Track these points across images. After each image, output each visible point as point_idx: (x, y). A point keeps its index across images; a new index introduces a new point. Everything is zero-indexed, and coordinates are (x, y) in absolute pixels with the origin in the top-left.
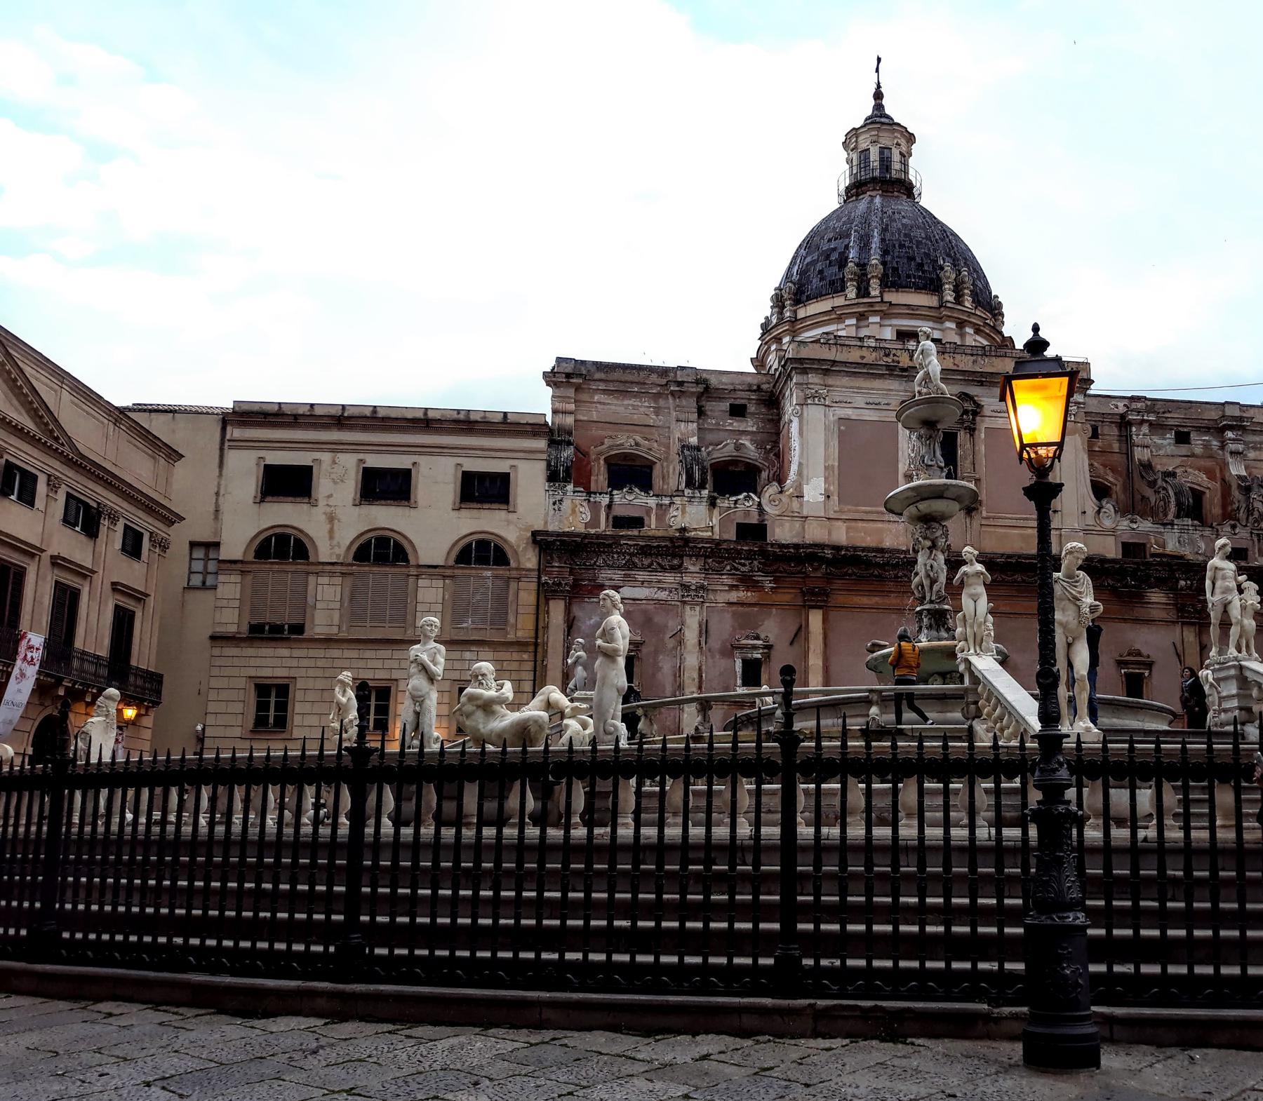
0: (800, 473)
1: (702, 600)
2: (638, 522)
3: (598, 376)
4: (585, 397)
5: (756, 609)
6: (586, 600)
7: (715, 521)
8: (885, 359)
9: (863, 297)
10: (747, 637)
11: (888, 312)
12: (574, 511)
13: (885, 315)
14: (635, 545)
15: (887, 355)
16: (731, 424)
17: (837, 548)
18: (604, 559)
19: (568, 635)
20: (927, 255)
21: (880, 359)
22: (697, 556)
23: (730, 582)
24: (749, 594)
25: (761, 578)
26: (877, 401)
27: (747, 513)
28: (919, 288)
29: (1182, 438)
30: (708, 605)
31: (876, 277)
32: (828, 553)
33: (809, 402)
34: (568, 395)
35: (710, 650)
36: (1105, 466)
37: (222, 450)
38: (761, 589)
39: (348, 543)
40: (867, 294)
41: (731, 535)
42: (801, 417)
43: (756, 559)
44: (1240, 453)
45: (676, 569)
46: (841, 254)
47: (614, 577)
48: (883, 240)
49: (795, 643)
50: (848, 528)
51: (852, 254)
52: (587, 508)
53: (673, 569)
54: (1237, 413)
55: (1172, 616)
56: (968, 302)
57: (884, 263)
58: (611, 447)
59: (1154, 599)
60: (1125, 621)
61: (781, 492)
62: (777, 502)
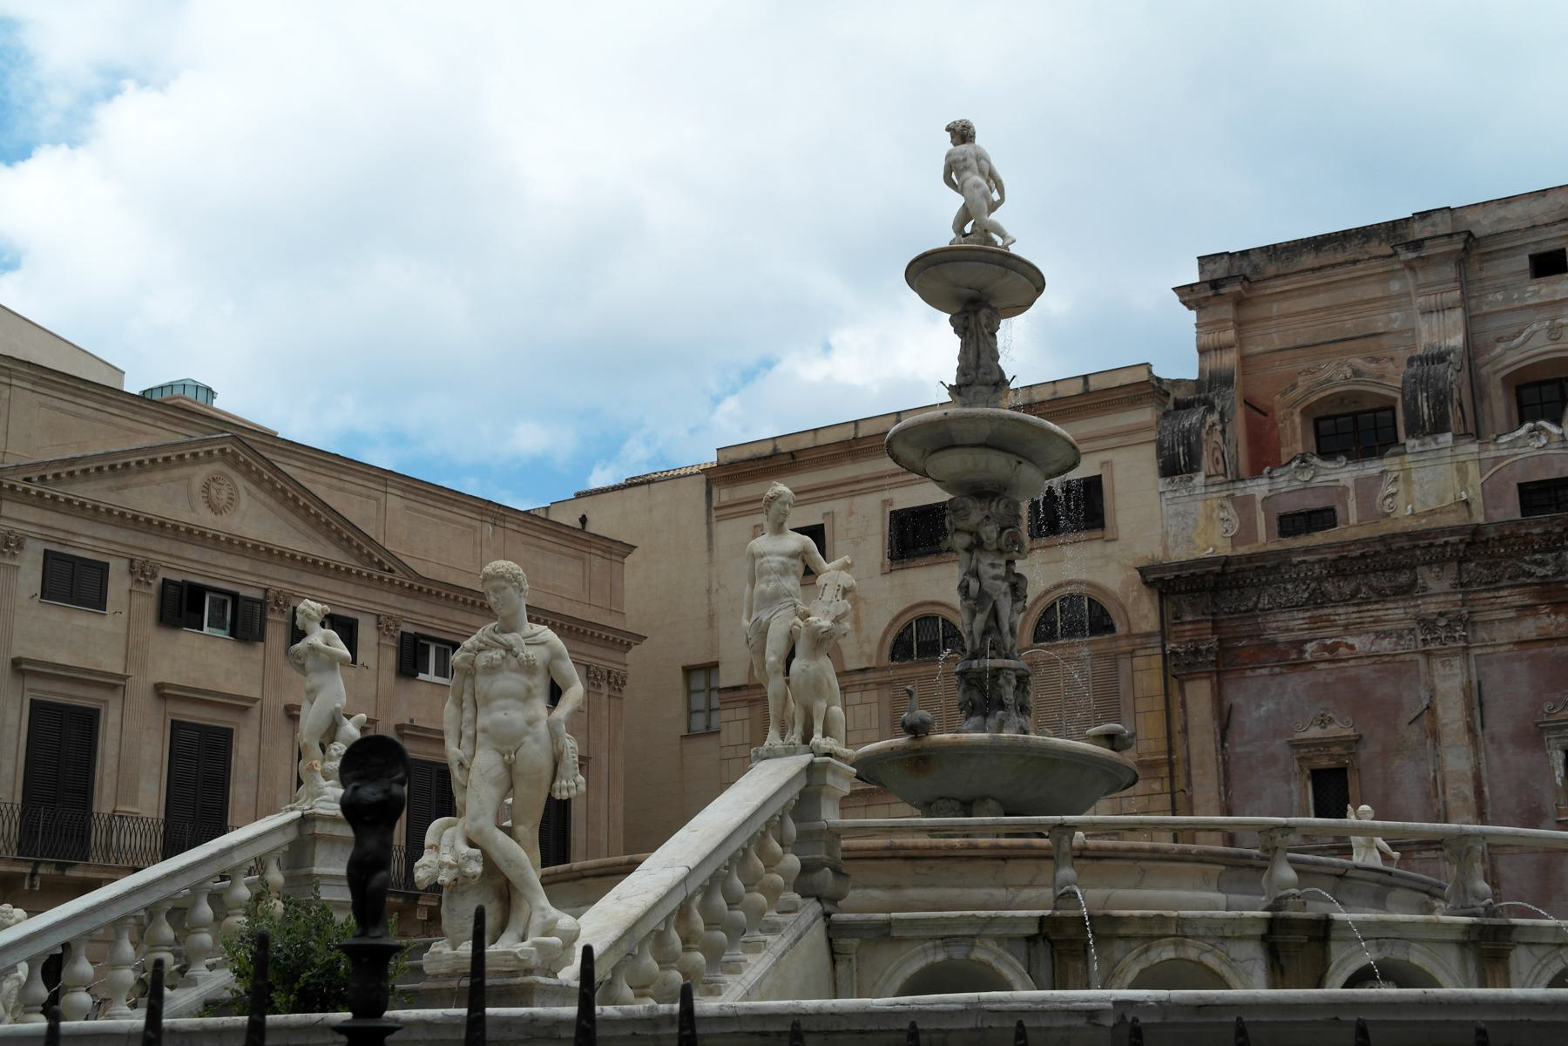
1: (1462, 644)
2: (1323, 518)
3: (1271, 270)
4: (1249, 313)
6: (1249, 673)
7: (1474, 493)
12: (1209, 518)
14: (1320, 561)
16: (1536, 293)
18: (1270, 596)
19: (1224, 738)
22: (1441, 561)
23: (1517, 600)
30: (1478, 651)
34: (1224, 317)
35: (1492, 740)
37: (709, 523)
39: (880, 634)
41: (1510, 509)
45: (1404, 593)
52: (1232, 510)
53: (1406, 591)
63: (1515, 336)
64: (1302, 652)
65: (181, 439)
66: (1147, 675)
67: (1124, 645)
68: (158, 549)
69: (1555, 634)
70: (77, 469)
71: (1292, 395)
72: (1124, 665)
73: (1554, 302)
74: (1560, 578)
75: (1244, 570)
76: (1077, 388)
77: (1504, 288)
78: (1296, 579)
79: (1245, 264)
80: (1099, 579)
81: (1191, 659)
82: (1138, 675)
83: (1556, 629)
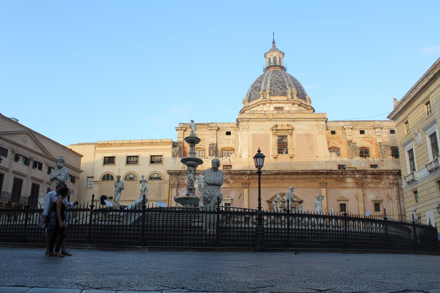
0: (241, 150)
5: (228, 189)
8: (265, 117)
10: (226, 197)
11: (271, 102)
12: (179, 164)
13: (270, 103)
15: (266, 116)
16: (226, 137)
17: (252, 171)
20: (283, 86)
21: (264, 117)
24: (227, 185)
25: (230, 180)
28: (281, 95)
29: (362, 132)
31: (268, 93)
32: (249, 172)
33: (243, 130)
36: (338, 142)
38: (229, 183)
40: (266, 98)
42: (241, 134)
44: (380, 136)
46: (259, 88)
48: (271, 83)
49: (240, 198)
51: (262, 87)
54: (379, 124)
55: (355, 185)
56: (295, 98)
59: (348, 181)
60: (339, 188)
61: (236, 156)
62: (234, 159)
63: (223, 143)
65: (21, 130)
66: (166, 187)
67: (163, 182)
68: (16, 148)
69: (225, 187)
70: (6, 133)
72: (163, 185)
73: (228, 139)
76: (160, 141)
77: (222, 136)
80: (160, 171)
81: (173, 185)
82: (165, 187)
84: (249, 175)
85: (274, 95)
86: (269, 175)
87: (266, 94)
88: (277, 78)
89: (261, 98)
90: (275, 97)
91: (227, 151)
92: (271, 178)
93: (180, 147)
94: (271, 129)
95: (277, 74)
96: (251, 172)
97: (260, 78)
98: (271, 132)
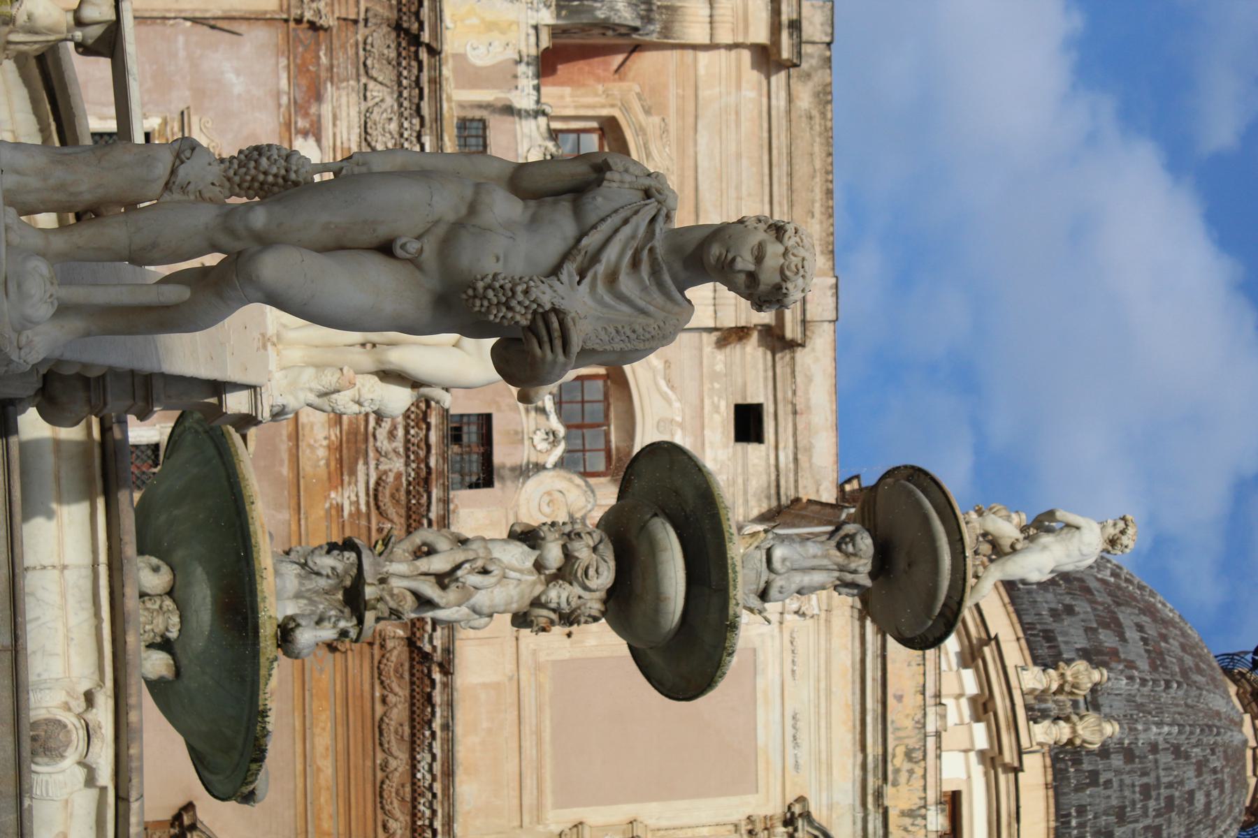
5: (285, 471)
8: (900, 751)
9: (1028, 708)
12: (491, 26)
13: (991, 760)
15: (909, 755)
16: (716, 409)
24: (322, 453)
26: (803, 737)
27: (517, 437)
31: (1074, 731)
34: (752, 29)
40: (1036, 715)
43: (407, 465)
46: (1114, 653)
47: (342, 126)
48: (1154, 748)
50: (497, 686)
52: (500, 58)
57: (1104, 752)
58: (640, 131)
63: (668, 381)
64: (305, 134)
69: (302, 445)
71: (636, 106)
73: (703, 428)
74: (371, 454)
75: (420, 69)
78: (401, 135)
79: (814, 62)
83: (311, 447)
84: (411, 643)
85: (1058, 784)
86: (414, 815)
87: (1067, 719)
88: (1191, 793)
89: (1033, 679)
90: (1041, 792)
91: (601, 419)
92: (385, 827)
93: (636, 29)
94: (797, 809)
95: (1222, 792)
96: (438, 656)
97: (1183, 647)
98: (775, 808)
